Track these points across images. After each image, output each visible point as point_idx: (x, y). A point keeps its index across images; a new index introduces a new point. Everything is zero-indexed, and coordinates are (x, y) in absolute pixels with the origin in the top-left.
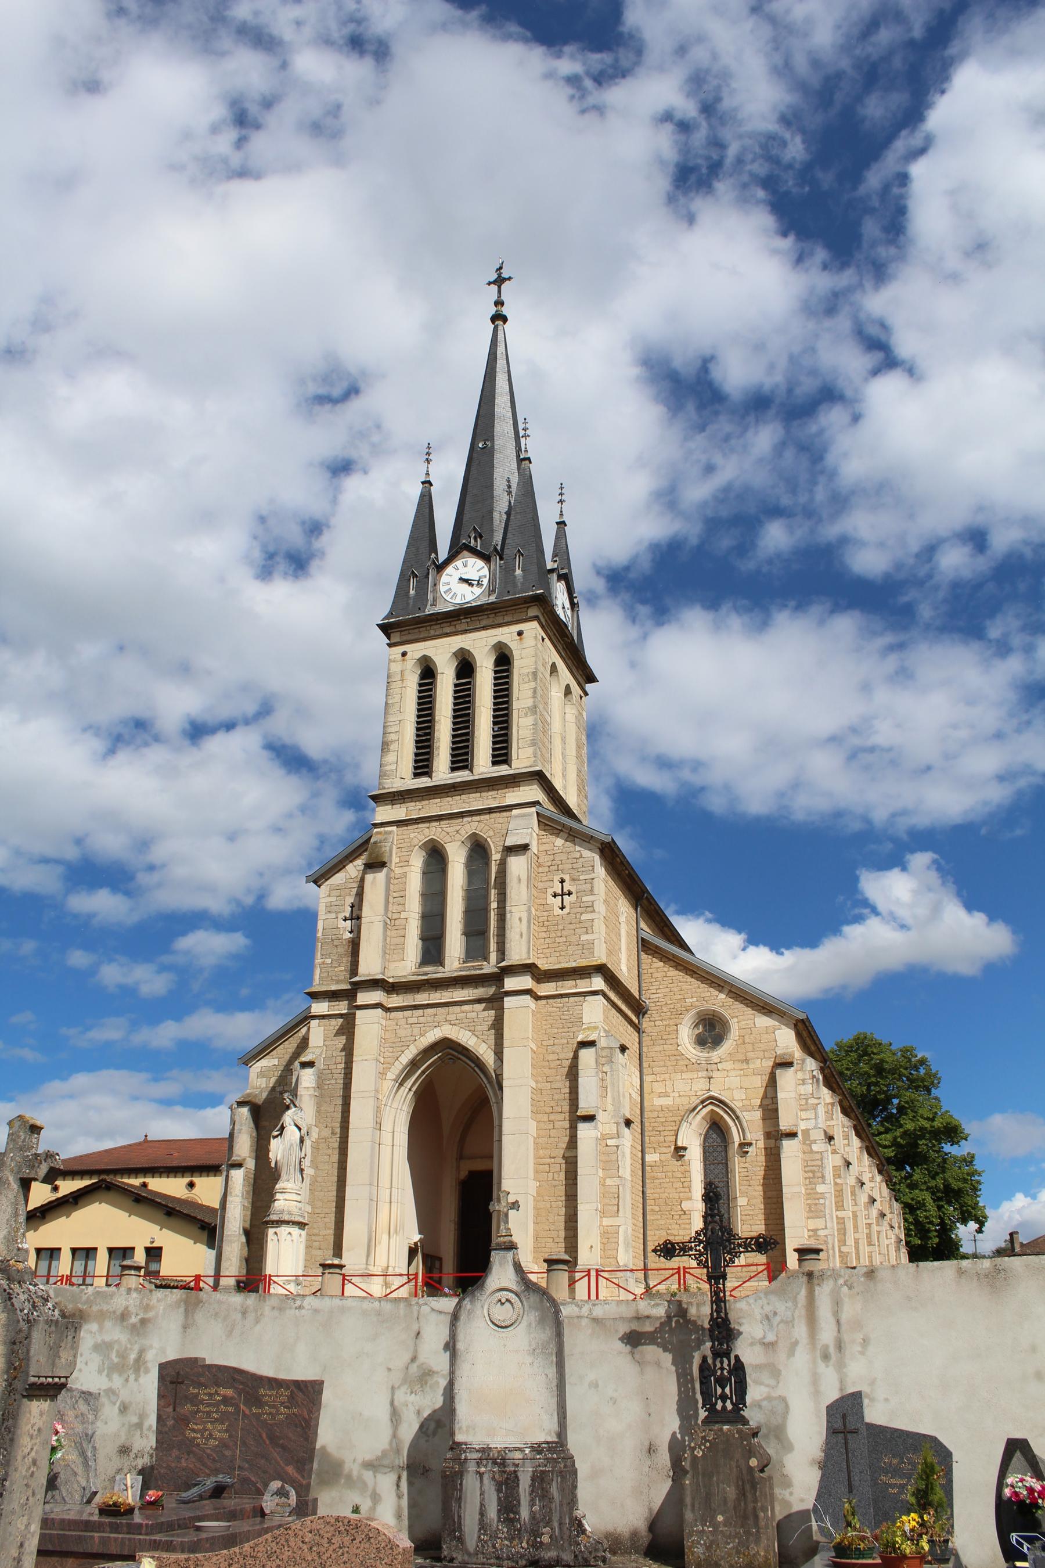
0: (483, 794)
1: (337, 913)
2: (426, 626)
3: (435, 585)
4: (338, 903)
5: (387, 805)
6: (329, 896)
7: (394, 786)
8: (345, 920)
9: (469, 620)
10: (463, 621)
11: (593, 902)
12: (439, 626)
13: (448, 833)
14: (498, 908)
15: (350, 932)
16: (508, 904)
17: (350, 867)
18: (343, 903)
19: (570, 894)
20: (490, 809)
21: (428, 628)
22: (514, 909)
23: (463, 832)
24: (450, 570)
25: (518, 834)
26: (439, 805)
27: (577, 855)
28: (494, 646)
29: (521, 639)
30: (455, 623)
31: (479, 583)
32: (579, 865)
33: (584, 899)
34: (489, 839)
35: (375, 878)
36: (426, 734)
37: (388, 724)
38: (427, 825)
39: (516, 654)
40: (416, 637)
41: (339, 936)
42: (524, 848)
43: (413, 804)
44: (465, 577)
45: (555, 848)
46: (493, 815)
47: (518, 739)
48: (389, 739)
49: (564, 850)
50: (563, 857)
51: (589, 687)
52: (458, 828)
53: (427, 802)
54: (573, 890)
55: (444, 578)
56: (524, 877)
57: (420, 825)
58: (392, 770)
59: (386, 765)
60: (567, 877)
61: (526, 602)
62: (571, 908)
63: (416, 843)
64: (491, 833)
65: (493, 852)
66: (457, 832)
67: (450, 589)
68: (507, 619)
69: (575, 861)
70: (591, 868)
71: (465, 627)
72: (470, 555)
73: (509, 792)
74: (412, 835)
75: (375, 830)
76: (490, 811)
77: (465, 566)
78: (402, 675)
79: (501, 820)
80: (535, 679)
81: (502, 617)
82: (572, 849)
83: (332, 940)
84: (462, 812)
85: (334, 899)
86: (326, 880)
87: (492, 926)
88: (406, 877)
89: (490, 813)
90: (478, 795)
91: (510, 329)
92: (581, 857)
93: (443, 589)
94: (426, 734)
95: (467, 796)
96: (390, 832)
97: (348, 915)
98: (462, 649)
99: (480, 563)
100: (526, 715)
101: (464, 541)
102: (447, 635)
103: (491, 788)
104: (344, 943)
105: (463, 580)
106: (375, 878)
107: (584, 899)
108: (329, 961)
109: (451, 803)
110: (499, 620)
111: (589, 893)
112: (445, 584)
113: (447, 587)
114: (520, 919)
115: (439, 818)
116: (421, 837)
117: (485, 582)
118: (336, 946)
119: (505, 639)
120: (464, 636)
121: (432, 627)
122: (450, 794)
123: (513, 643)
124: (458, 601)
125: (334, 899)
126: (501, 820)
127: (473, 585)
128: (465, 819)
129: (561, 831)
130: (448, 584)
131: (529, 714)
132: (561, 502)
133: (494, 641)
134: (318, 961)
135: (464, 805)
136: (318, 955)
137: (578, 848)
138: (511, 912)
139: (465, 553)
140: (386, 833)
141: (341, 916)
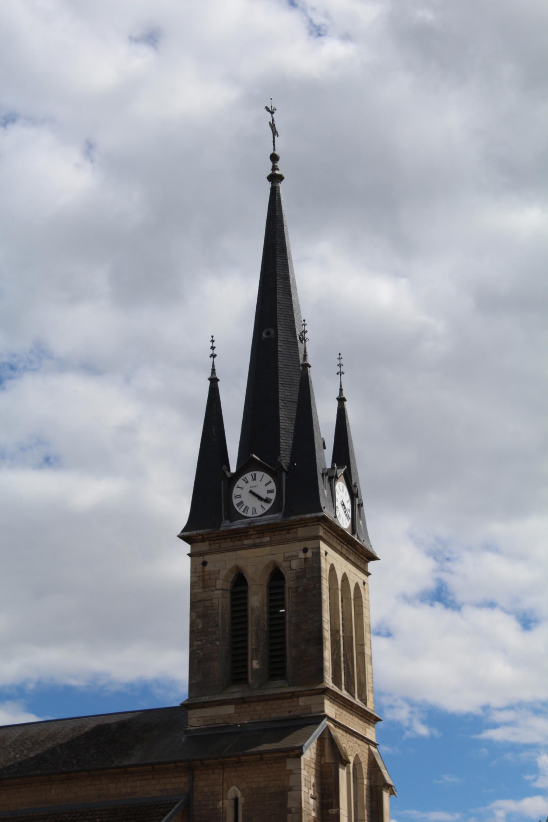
24: (240, 482)
31: (267, 501)
51: (371, 566)
55: (236, 491)
77: (254, 479)
91: (283, 187)
93: (235, 501)
124: (249, 514)
130: (240, 496)
132: (340, 359)
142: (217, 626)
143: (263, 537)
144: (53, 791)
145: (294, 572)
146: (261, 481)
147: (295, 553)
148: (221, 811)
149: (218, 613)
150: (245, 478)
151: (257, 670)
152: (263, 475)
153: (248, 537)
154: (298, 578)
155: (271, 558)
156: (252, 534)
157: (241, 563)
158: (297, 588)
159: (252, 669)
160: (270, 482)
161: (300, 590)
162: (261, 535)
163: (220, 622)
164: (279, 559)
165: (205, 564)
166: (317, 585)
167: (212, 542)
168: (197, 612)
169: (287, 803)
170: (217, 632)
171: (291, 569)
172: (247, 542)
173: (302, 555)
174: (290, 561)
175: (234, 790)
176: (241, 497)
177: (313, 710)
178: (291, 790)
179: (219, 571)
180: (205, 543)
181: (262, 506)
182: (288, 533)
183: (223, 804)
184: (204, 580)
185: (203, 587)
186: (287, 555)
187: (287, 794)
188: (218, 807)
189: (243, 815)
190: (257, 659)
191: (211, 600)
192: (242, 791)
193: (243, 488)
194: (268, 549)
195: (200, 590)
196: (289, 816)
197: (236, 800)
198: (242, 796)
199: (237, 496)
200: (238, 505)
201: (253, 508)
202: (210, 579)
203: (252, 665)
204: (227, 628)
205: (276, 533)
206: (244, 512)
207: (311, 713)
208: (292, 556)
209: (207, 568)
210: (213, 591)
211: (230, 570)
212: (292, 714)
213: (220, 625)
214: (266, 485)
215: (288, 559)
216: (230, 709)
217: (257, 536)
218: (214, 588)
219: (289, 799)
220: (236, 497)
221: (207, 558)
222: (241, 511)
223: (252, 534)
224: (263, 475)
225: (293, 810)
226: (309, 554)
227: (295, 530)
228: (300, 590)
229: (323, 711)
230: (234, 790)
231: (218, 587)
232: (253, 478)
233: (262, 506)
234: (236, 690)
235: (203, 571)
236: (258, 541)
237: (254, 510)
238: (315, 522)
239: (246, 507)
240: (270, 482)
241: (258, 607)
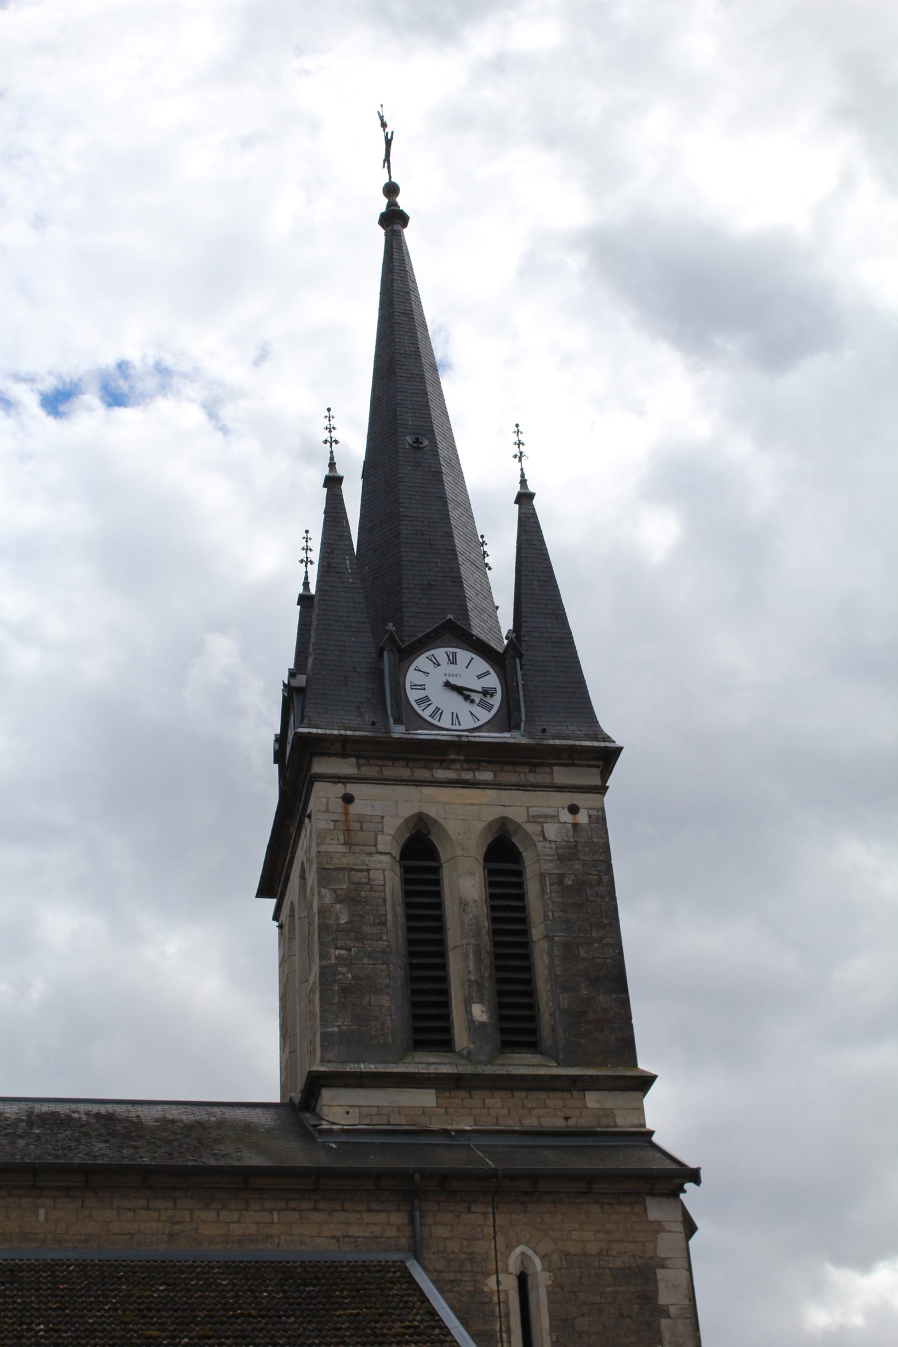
44: (453, 681)
55: (412, 677)
67: (426, 699)
77: (453, 661)
93: (413, 696)
99: (481, 665)
101: (450, 616)
105: (447, 685)
112: (414, 687)
113: (420, 694)
117: (496, 701)
124: (446, 722)
127: (472, 701)
130: (422, 687)
142: (384, 924)
143: (478, 769)
144: (42, 1212)
145: (553, 845)
146: (467, 667)
147: (550, 811)
148: (495, 1299)
149: (385, 900)
150: (433, 655)
151: (482, 1025)
152: (472, 659)
153: (445, 763)
154: (561, 859)
155: (497, 812)
156: (454, 761)
157: (431, 811)
158: (561, 877)
159: (471, 1020)
160: (488, 673)
161: (568, 882)
162: (474, 766)
163: (389, 917)
164: (518, 815)
165: (348, 799)
166: (605, 878)
167: (361, 761)
168: (334, 891)
169: (656, 1292)
170: (385, 937)
171: (545, 839)
172: (441, 774)
173: (566, 817)
174: (542, 823)
175: (523, 1253)
176: (424, 689)
177: (619, 1120)
178: (663, 1267)
179: (383, 817)
180: (347, 760)
181: (472, 714)
182: (531, 771)
183: (498, 1283)
184: (348, 831)
185: (345, 844)
186: (534, 811)
187: (655, 1273)
188: (486, 1289)
189: (551, 1312)
190: (481, 1002)
191: (368, 870)
192: (544, 1257)
193: (428, 674)
194: (490, 794)
195: (342, 848)
196: (664, 1323)
197: (523, 1280)
198: (544, 1270)
199: (416, 685)
200: (419, 702)
201: (453, 713)
202: (362, 829)
203: (469, 1012)
204: (400, 932)
205: (507, 768)
206: (432, 716)
207: (616, 1126)
208: (546, 816)
209: (354, 808)
210: (370, 854)
211: (407, 821)
212: (571, 1122)
213: (389, 924)
214: (479, 677)
215: (540, 820)
216: (426, 1098)
217: (465, 766)
218: (373, 849)
219: (661, 1285)
220: (412, 687)
221: (352, 789)
222: (426, 715)
223: (454, 761)
224: (472, 659)
225: (673, 1310)
226: (582, 818)
227: (548, 769)
228: (568, 882)
229: (644, 1125)
230: (523, 1253)
231: (381, 847)
232: (449, 659)
233: (472, 714)
234: (432, 1060)
235: (346, 813)
236: (467, 776)
237: (455, 717)
238: (592, 760)
239: (438, 709)
240: (488, 673)
241: (476, 901)
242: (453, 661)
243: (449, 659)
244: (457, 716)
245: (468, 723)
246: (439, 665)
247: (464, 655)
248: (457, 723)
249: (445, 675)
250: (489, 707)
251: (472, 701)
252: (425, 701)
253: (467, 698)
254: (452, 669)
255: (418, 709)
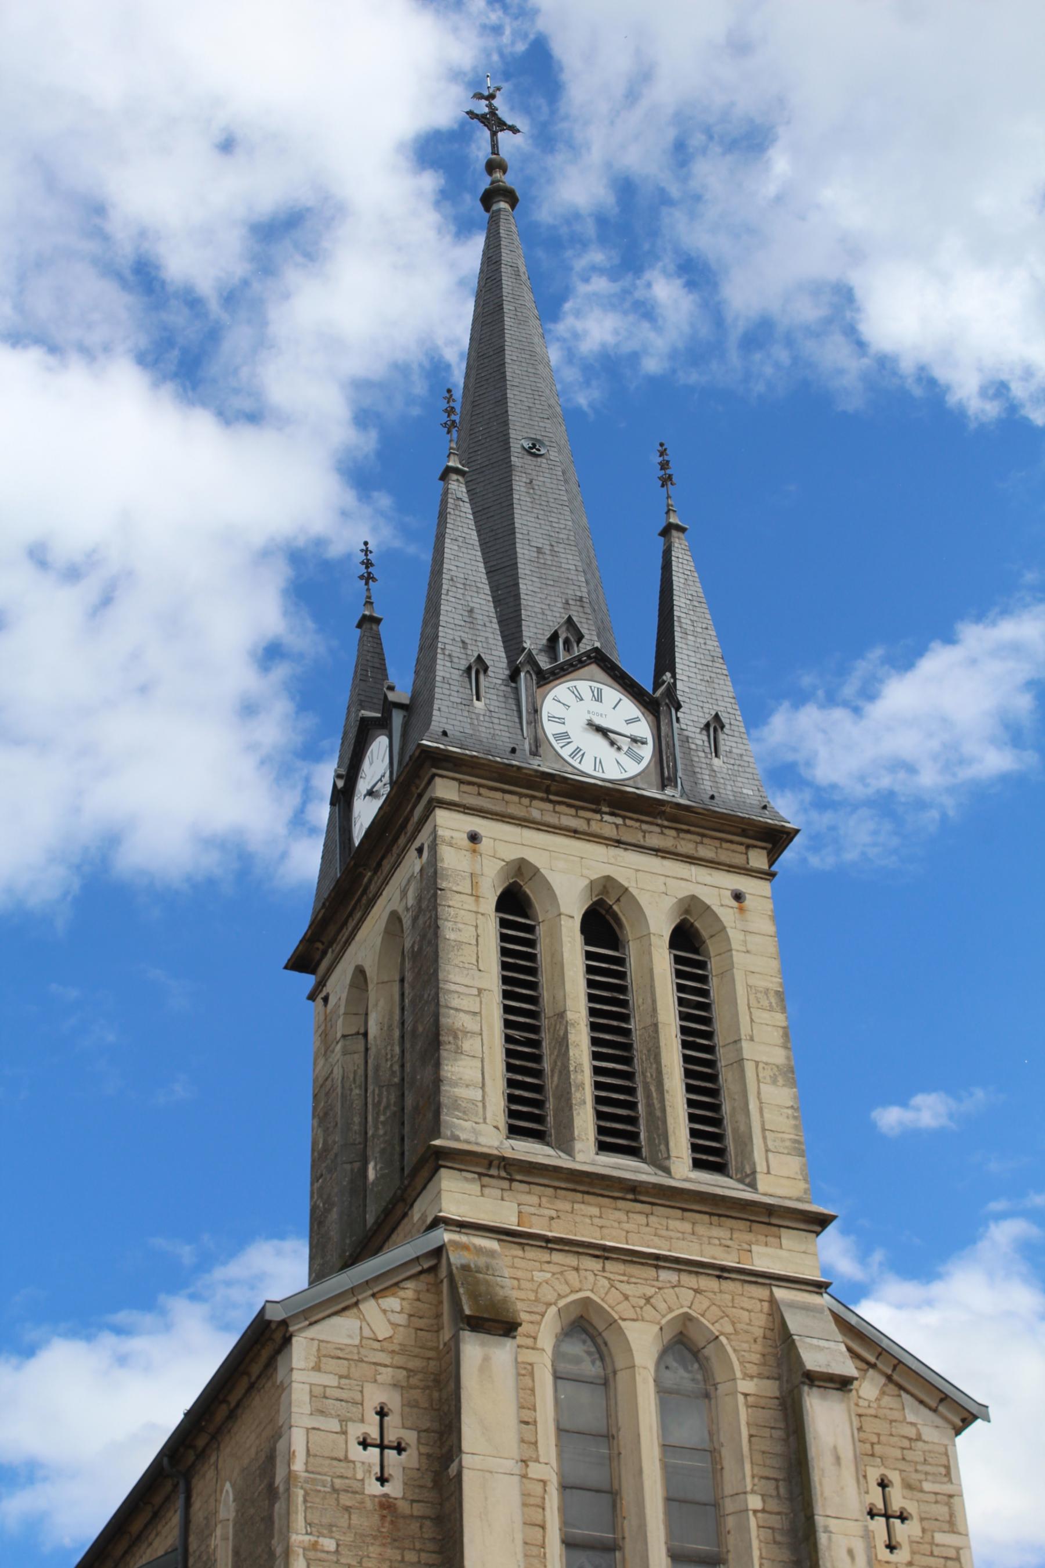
0: (701, 1230)
1: (343, 1421)
2: (521, 795)
3: (536, 711)
4: (344, 1395)
5: (466, 1179)
6: (317, 1368)
7: (482, 1140)
8: (365, 1444)
9: (619, 821)
10: (606, 818)
11: (958, 1549)
12: (550, 806)
13: (626, 1297)
14: (763, 1511)
15: (382, 1480)
16: (819, 1509)
17: (370, 1308)
18: (358, 1397)
19: (903, 1517)
20: (723, 1269)
21: (526, 801)
22: (833, 1524)
23: (662, 1306)
25: (821, 1349)
26: (596, 1221)
27: (912, 1432)
28: (681, 901)
29: (741, 910)
30: (589, 815)
32: (916, 1456)
33: (939, 1538)
34: (722, 1339)
35: (486, 1359)
36: (529, 1043)
37: (453, 987)
38: (572, 1260)
39: (735, 936)
40: (498, 808)
41: (356, 1485)
42: (843, 1384)
43: (534, 1200)
44: (598, 721)
45: (861, 1403)
46: (727, 1285)
47: (764, 1130)
48: (458, 1025)
49: (881, 1413)
50: (882, 1427)
52: (650, 1291)
53: (567, 1206)
54: (911, 1508)
56: (847, 1453)
57: (557, 1257)
58: (473, 1102)
59: (455, 1084)
60: (894, 1477)
61: (744, 833)
62: (913, 1553)
63: (551, 1297)
64: (729, 1329)
65: (739, 1374)
66: (648, 1300)
67: (565, 736)
68: (705, 852)
69: (906, 1443)
70: (943, 1471)
71: (609, 831)
72: (609, 680)
73: (757, 1243)
74: (539, 1276)
75: (448, 1236)
76: (722, 1272)
77: (598, 698)
78: (474, 885)
79: (747, 1303)
80: (784, 1010)
81: (692, 846)
82: (896, 1415)
83: (335, 1490)
84: (657, 1257)
85: (331, 1381)
86: (311, 1324)
87: (756, 1553)
88: (532, 1374)
89: (719, 1277)
90: (687, 1227)
92: (919, 1438)
93: (550, 729)
94: (529, 1043)
95: (664, 1222)
96: (492, 1254)
97: (374, 1434)
98: (608, 879)
99: (630, 708)
100: (774, 1081)
102: (574, 833)
103: (715, 1219)
104: (369, 1504)
106: (486, 1359)
107: (939, 1538)
108: (329, 1544)
109: (626, 1226)
110: (686, 846)
111: (946, 1527)
112: (551, 718)
113: (559, 729)
114: (850, 1552)
115: (604, 1253)
116: (564, 1289)
117: (647, 752)
118: (347, 1509)
119: (708, 897)
120: (613, 852)
121: (535, 803)
122: (621, 1204)
123: (727, 914)
124: (587, 767)
125: (331, 1381)
126: (747, 1303)
127: (619, 749)
128: (664, 1275)
129: (873, 1366)
130: (562, 721)
131: (781, 1081)
133: (684, 890)
134: (299, 1538)
135: (656, 1239)
136: (299, 1521)
137: (911, 1417)
138: (826, 1530)
139: (593, 669)
140: (479, 1251)
141: (356, 1431)
146: (614, 708)
152: (620, 700)
176: (564, 723)
181: (618, 762)
200: (558, 737)
201: (596, 758)
206: (573, 755)
214: (629, 722)
222: (565, 753)
224: (620, 700)
232: (594, 695)
233: (618, 762)
239: (578, 750)
242: (598, 698)
243: (594, 695)
244: (600, 762)
245: (612, 773)
246: (582, 699)
247: (612, 694)
248: (601, 770)
249: (589, 712)
250: (639, 759)
251: (619, 749)
252: (565, 736)
253: (612, 743)
254: (596, 706)
255: (557, 747)
